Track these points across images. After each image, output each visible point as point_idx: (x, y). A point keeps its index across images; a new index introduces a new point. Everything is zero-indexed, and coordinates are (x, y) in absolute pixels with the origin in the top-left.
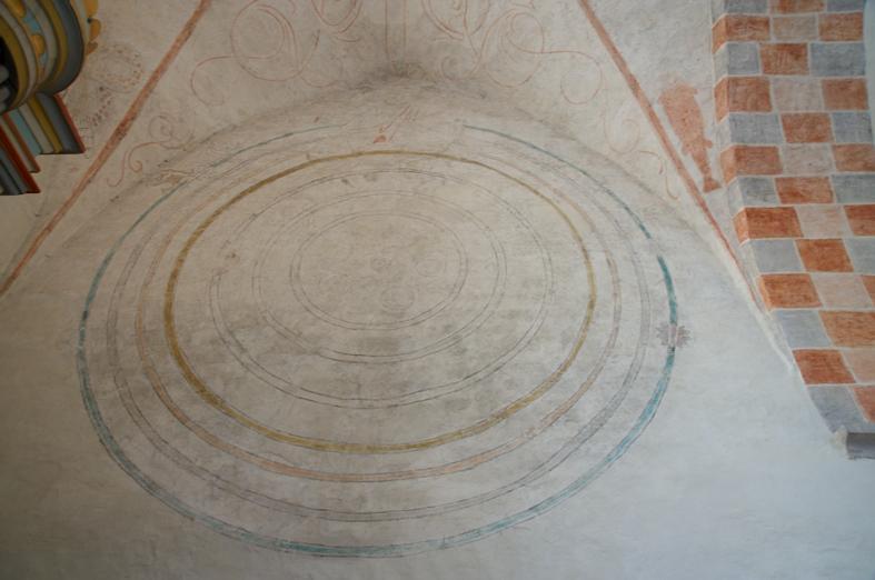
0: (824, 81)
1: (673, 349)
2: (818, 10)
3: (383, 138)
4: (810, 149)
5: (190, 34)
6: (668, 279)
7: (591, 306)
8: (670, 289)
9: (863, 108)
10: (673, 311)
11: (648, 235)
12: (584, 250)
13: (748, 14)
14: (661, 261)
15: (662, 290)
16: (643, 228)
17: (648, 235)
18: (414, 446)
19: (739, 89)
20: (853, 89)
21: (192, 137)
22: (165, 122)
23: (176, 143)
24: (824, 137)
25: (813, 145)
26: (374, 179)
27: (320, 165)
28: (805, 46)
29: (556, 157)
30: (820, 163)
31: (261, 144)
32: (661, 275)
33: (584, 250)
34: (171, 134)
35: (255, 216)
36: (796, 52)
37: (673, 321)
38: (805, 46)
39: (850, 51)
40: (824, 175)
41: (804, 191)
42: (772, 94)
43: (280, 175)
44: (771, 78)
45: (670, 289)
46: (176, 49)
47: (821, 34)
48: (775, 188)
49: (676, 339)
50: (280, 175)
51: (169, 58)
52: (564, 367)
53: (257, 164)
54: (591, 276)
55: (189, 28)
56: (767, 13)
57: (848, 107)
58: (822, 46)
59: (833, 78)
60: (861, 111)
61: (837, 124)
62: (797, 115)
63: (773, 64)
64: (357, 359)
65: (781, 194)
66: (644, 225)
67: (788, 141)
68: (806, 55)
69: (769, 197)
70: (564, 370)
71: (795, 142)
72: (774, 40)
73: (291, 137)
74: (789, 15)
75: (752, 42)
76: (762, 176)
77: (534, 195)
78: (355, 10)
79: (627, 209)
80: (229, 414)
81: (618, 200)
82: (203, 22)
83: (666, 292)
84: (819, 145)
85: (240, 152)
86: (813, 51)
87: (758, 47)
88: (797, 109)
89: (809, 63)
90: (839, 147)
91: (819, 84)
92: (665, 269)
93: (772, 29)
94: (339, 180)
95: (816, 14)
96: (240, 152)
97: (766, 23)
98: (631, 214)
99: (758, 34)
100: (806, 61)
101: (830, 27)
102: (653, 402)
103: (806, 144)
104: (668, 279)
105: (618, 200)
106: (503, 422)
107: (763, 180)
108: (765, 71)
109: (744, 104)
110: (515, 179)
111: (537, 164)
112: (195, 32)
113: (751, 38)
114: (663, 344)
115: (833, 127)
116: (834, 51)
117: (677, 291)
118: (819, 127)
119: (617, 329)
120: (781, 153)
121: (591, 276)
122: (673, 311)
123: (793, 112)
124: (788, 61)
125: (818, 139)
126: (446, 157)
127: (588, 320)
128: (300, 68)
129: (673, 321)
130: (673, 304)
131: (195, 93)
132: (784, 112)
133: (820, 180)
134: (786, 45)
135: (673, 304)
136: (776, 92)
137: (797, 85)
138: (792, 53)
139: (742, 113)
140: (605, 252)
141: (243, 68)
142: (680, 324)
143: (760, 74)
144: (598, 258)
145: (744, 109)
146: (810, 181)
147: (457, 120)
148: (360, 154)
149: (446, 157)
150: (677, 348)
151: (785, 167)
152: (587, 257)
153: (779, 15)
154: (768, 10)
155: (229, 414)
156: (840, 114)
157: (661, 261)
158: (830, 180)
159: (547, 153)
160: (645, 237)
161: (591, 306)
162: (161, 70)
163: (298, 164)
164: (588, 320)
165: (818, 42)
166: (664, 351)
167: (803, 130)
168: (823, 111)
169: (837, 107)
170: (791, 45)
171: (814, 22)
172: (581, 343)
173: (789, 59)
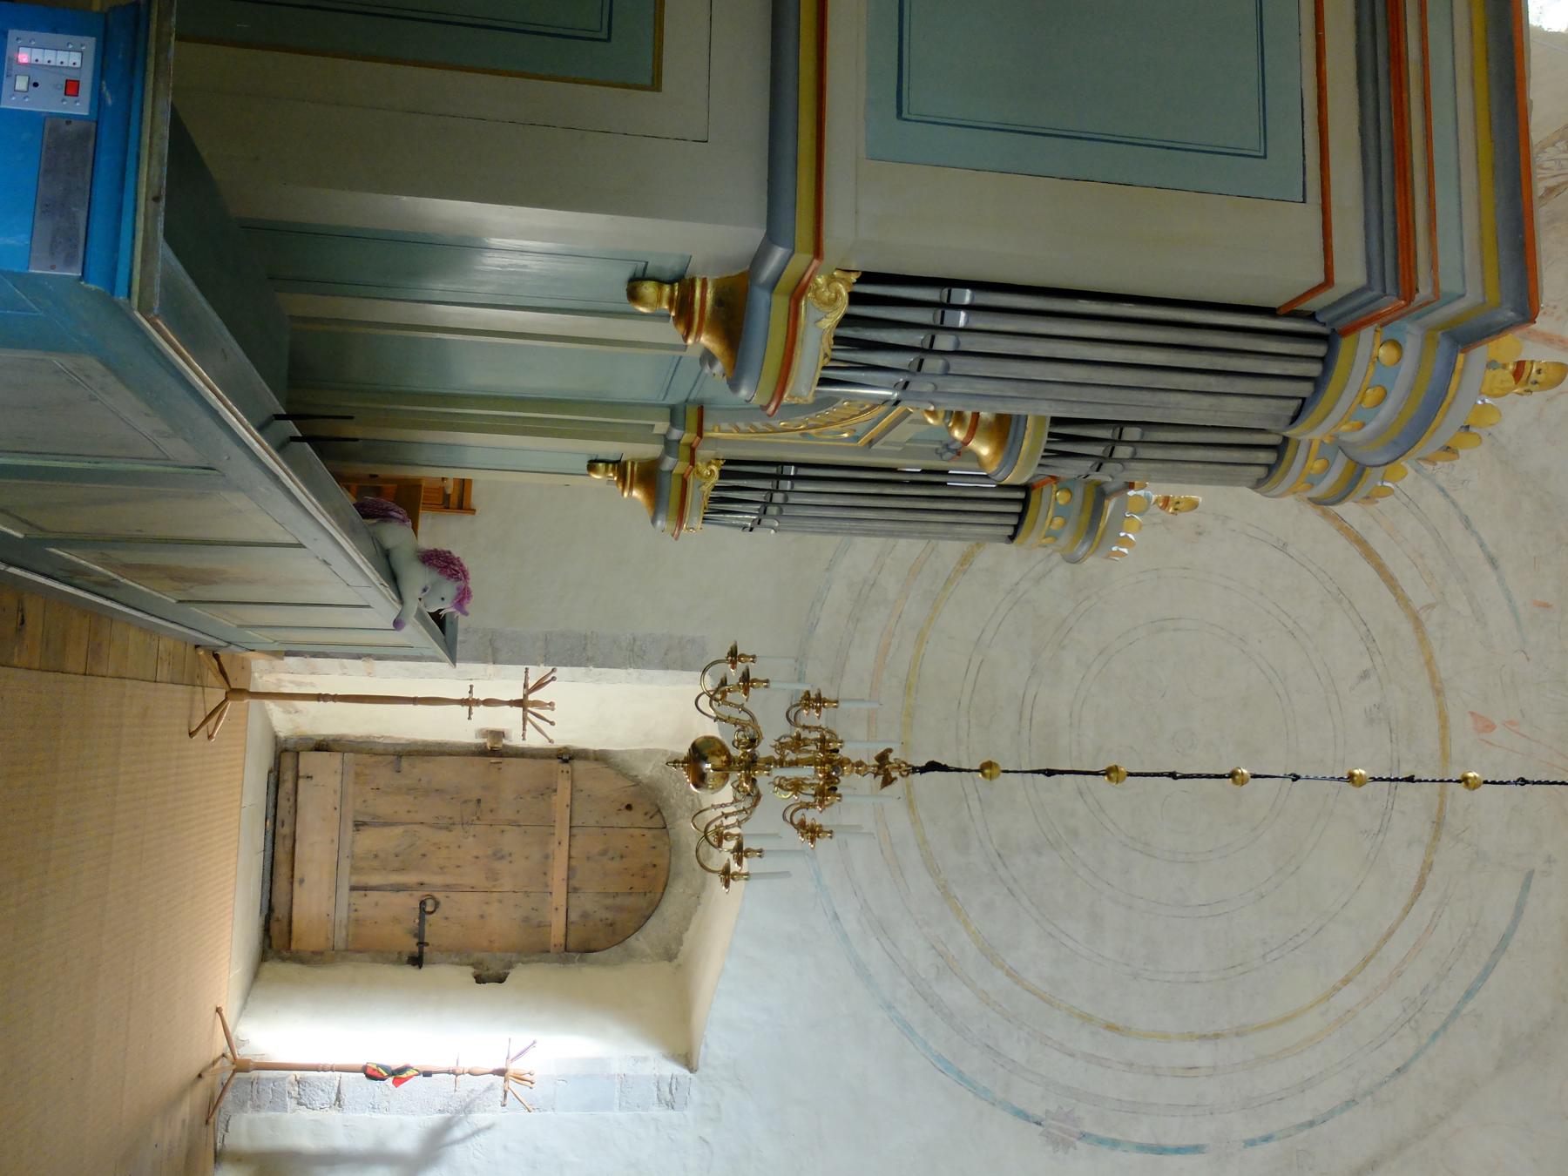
1: (1039, 1123)
3: (1490, 727)
6: (1161, 1150)
7: (1110, 1027)
8: (1143, 1148)
10: (1101, 1141)
11: (1251, 1143)
12: (1217, 1036)
14: (1196, 1149)
15: (1142, 1132)
16: (1267, 1139)
17: (1251, 1143)
18: (909, 792)
26: (1371, 721)
27: (1406, 628)
29: (1444, 1027)
31: (1467, 522)
32: (1169, 1141)
33: (1217, 1036)
35: (1283, 548)
37: (1083, 1136)
43: (1380, 568)
45: (1143, 1148)
49: (1056, 1132)
50: (1380, 568)
52: (1010, 973)
54: (1165, 1037)
64: (1026, 723)
66: (1273, 1144)
70: (1008, 974)
73: (1487, 568)
77: (1342, 975)
79: (1311, 1124)
80: (949, 581)
81: (1331, 1113)
83: (1136, 1139)
85: (1442, 490)
92: (1179, 1150)
94: (1366, 664)
96: (1442, 490)
98: (1301, 1127)
102: (960, 1074)
104: (1161, 1150)
105: (1331, 1113)
106: (938, 893)
110: (1378, 949)
111: (1424, 991)
114: (1047, 1112)
117: (1137, 1157)
119: (1072, 1055)
121: (1165, 1037)
122: (1101, 1141)
126: (1436, 837)
127: (1086, 1019)
129: (1083, 1136)
130: (1115, 1144)
135: (1115, 1144)
140: (1215, 1068)
142: (1079, 1144)
144: (1203, 1055)
147: (1549, 860)
148: (1438, 692)
149: (1436, 837)
150: (1040, 1129)
152: (1203, 1037)
155: (949, 581)
157: (1196, 1149)
159: (1455, 1013)
160: (1250, 1136)
161: (1110, 1027)
163: (1409, 594)
164: (1086, 1019)
166: (1038, 1111)
172: (1049, 1002)
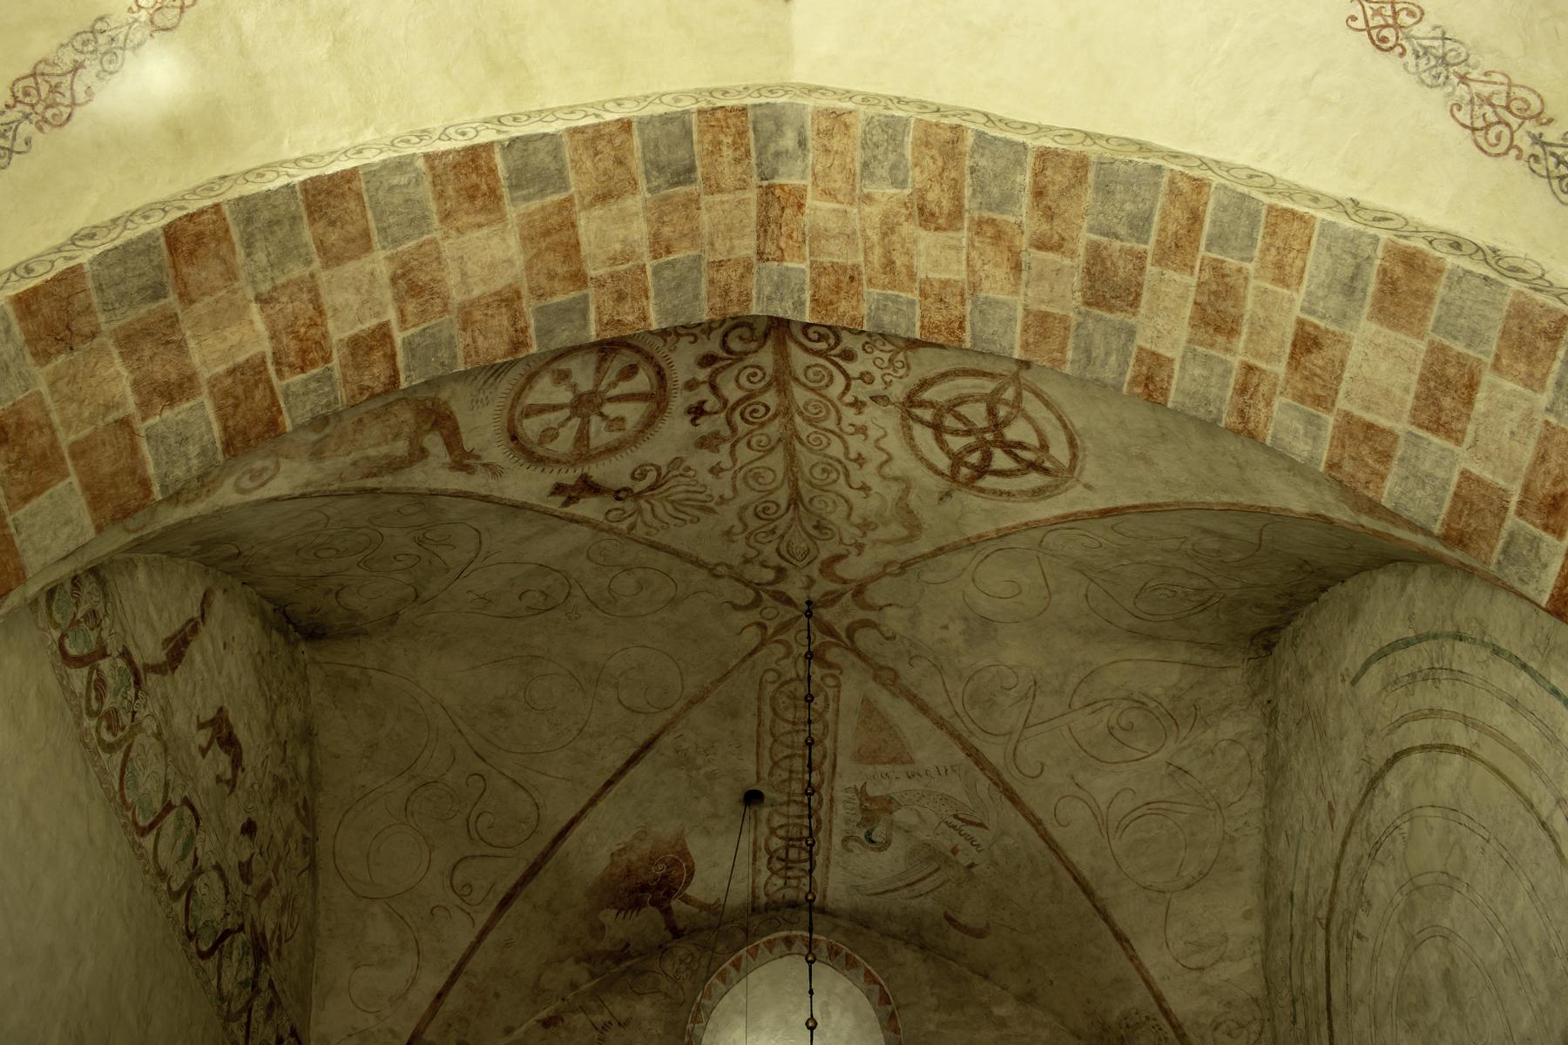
0: (1370, 318)
2: (1246, 279)
4: (1486, 415)
5: (1128, 941)
9: (1440, 271)
13: (1230, 392)
19: (1348, 467)
20: (1399, 271)
21: (1255, 1000)
22: (1224, 1027)
23: (1255, 1027)
24: (1472, 375)
25: (1480, 406)
28: (1301, 323)
30: (1515, 415)
34: (1241, 1026)
36: (1306, 342)
38: (1301, 323)
39: (1329, 249)
40: (1538, 428)
41: (1555, 484)
42: (1369, 417)
44: (1342, 404)
46: (1139, 967)
47: (1288, 286)
48: (1531, 527)
51: (1148, 983)
53: (1309, 981)
55: (1120, 937)
56: (1235, 362)
57: (1430, 297)
58: (1309, 293)
59: (1369, 300)
60: (1444, 280)
61: (1456, 338)
62: (1417, 397)
63: (1319, 392)
65: (1546, 528)
67: (1458, 442)
68: (1316, 327)
69: (1544, 551)
71: (1463, 432)
72: (1280, 369)
74: (1245, 330)
75: (1276, 406)
76: (1504, 533)
78: (1152, 705)
82: (1117, 916)
84: (1481, 395)
86: (1313, 313)
87: (1284, 400)
88: (1406, 390)
89: (1333, 327)
90: (1498, 357)
91: (1374, 327)
93: (1262, 365)
95: (1253, 283)
97: (1250, 369)
99: (1264, 388)
100: (1327, 331)
101: (1279, 266)
103: (1473, 414)
107: (1512, 535)
108: (1328, 410)
109: (1374, 472)
112: (1127, 932)
113: (1269, 404)
115: (1459, 347)
116: (1323, 276)
118: (1451, 371)
120: (1475, 469)
123: (1410, 400)
124: (1320, 363)
125: (1472, 386)
128: (1213, 804)
131: (1201, 969)
132: (1406, 416)
133: (1546, 438)
134: (1292, 356)
136: (1368, 409)
137: (1365, 368)
138: (1309, 351)
139: (1388, 484)
141: (1188, 887)
143: (1330, 420)
145: (1383, 478)
146: (1542, 458)
151: (1502, 483)
153: (1241, 342)
154: (1228, 357)
156: (1438, 319)
158: (1553, 420)
162: (1159, 999)
165: (1300, 298)
167: (1447, 402)
168: (1422, 346)
169: (1425, 318)
170: (1294, 345)
171: (1265, 291)
173: (1316, 360)
